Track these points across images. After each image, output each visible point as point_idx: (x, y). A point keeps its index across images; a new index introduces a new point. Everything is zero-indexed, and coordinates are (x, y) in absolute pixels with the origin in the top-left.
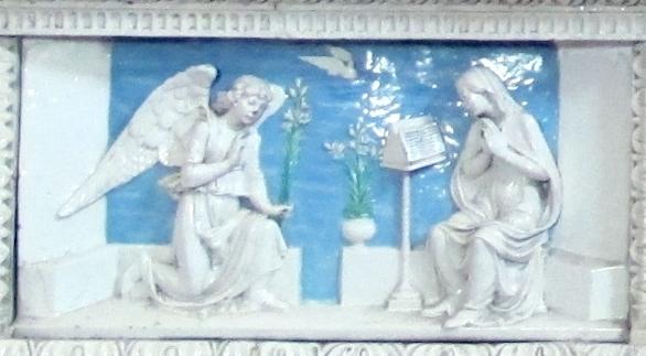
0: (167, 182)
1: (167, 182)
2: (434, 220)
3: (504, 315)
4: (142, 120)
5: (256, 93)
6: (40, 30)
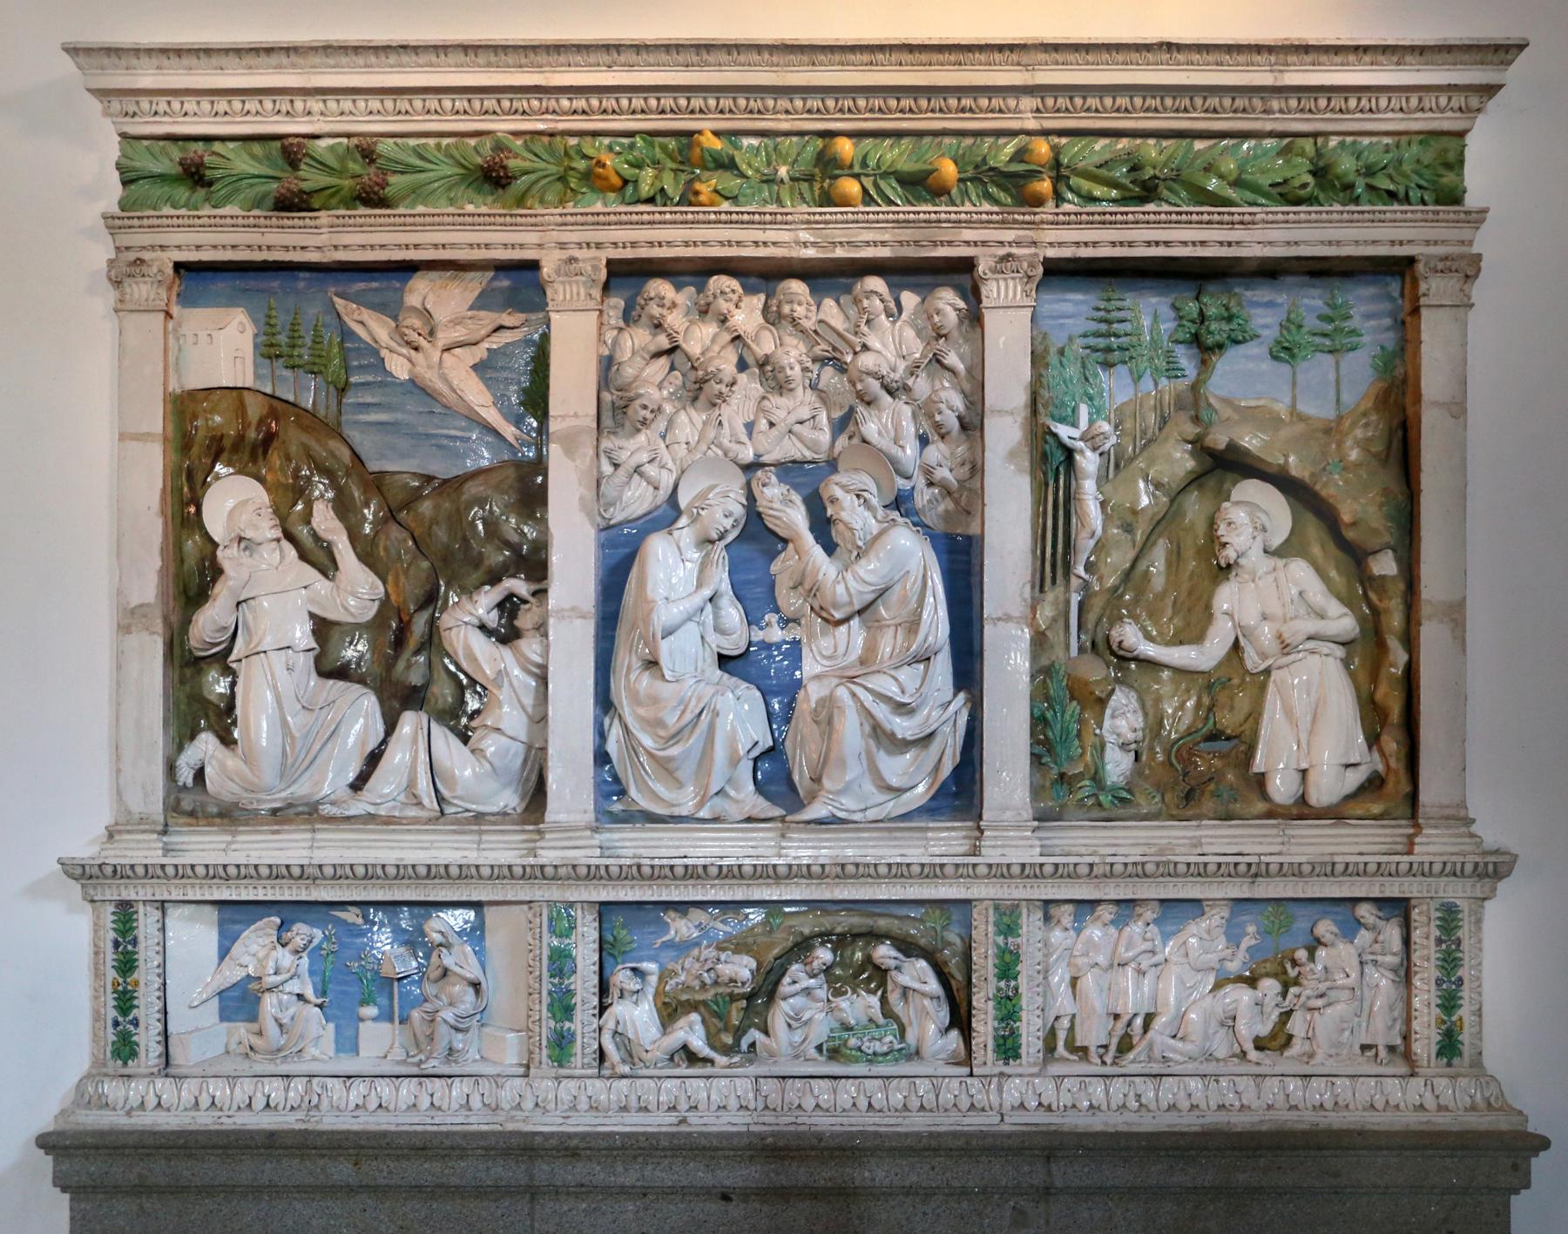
0: (253, 986)
1: (253, 986)
2: (413, 1008)
3: (456, 1062)
4: (237, 949)
5: (301, 932)
6: (173, 897)
